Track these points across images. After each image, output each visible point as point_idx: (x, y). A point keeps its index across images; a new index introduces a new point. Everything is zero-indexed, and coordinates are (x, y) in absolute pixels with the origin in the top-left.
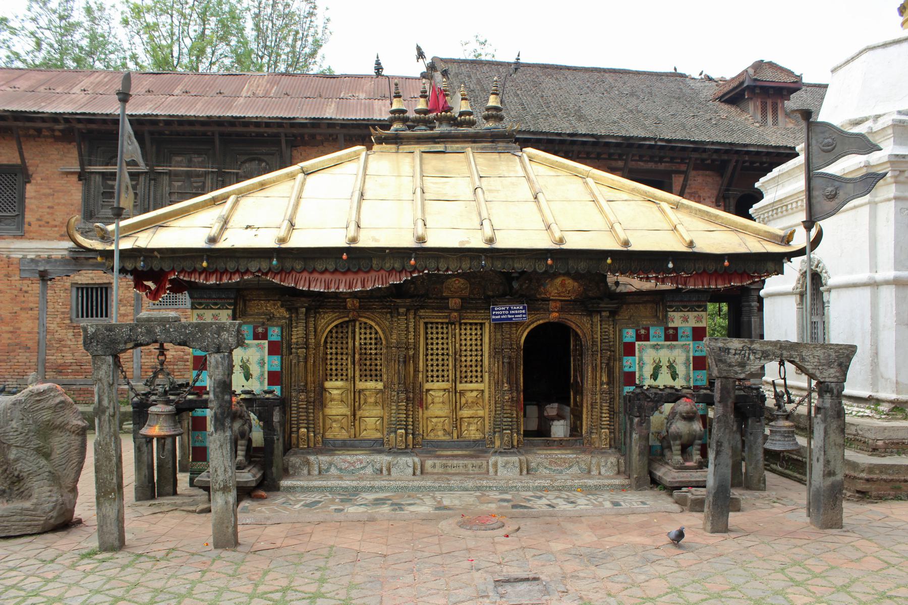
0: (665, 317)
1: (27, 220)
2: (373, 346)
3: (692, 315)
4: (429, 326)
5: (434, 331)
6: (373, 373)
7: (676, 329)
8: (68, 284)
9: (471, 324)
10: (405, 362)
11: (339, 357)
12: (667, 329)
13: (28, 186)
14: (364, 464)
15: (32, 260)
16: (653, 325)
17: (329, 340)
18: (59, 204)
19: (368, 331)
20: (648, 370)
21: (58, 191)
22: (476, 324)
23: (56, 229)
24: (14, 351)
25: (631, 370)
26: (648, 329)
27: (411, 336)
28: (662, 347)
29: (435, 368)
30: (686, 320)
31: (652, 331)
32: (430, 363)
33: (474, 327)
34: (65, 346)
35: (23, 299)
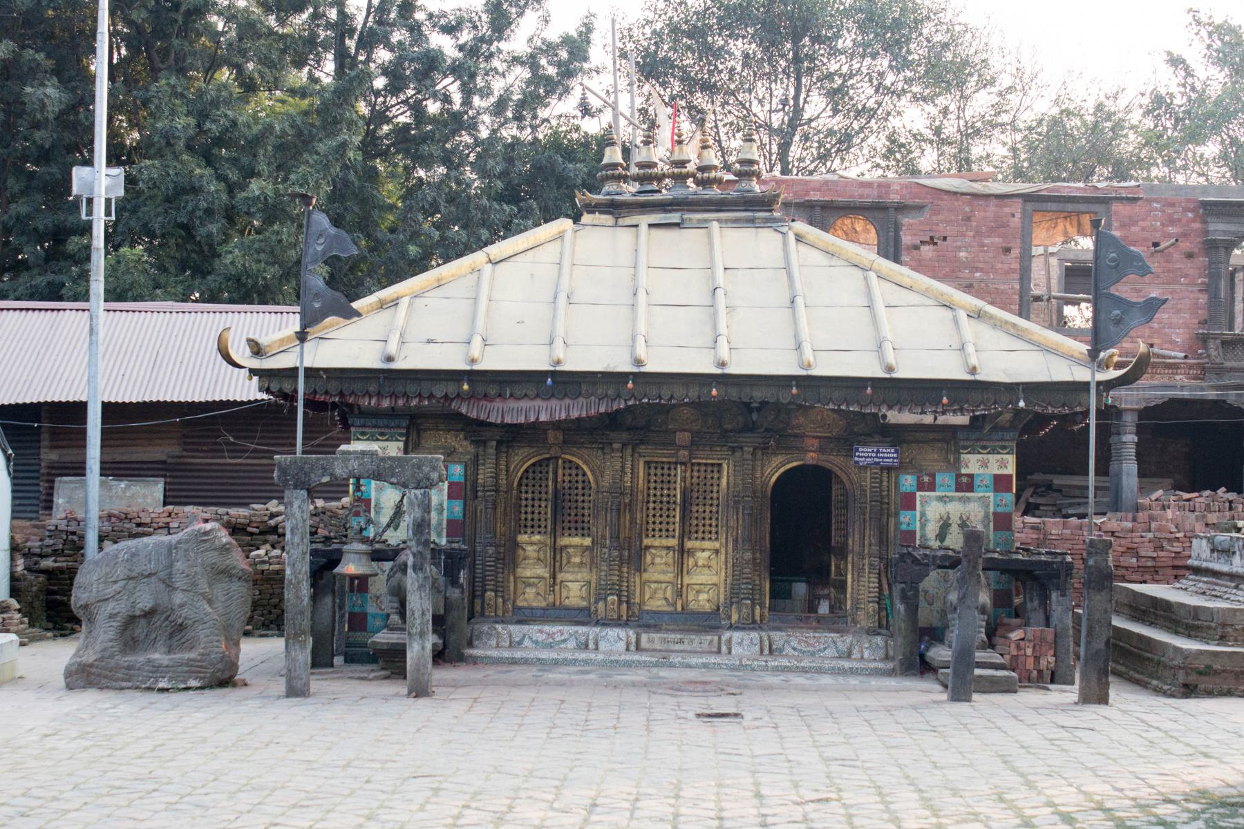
0: (958, 460)
2: (580, 491)
3: (993, 458)
4: (653, 465)
5: (659, 472)
6: (579, 525)
7: (971, 476)
9: (706, 464)
10: (619, 510)
11: (537, 503)
12: (959, 476)
14: (566, 636)
16: (940, 471)
17: (525, 481)
19: (574, 472)
20: (932, 529)
22: (713, 465)
25: (911, 528)
26: (933, 476)
27: (628, 478)
28: (952, 499)
29: (658, 520)
30: (985, 464)
31: (939, 478)
32: (651, 512)
33: (710, 469)
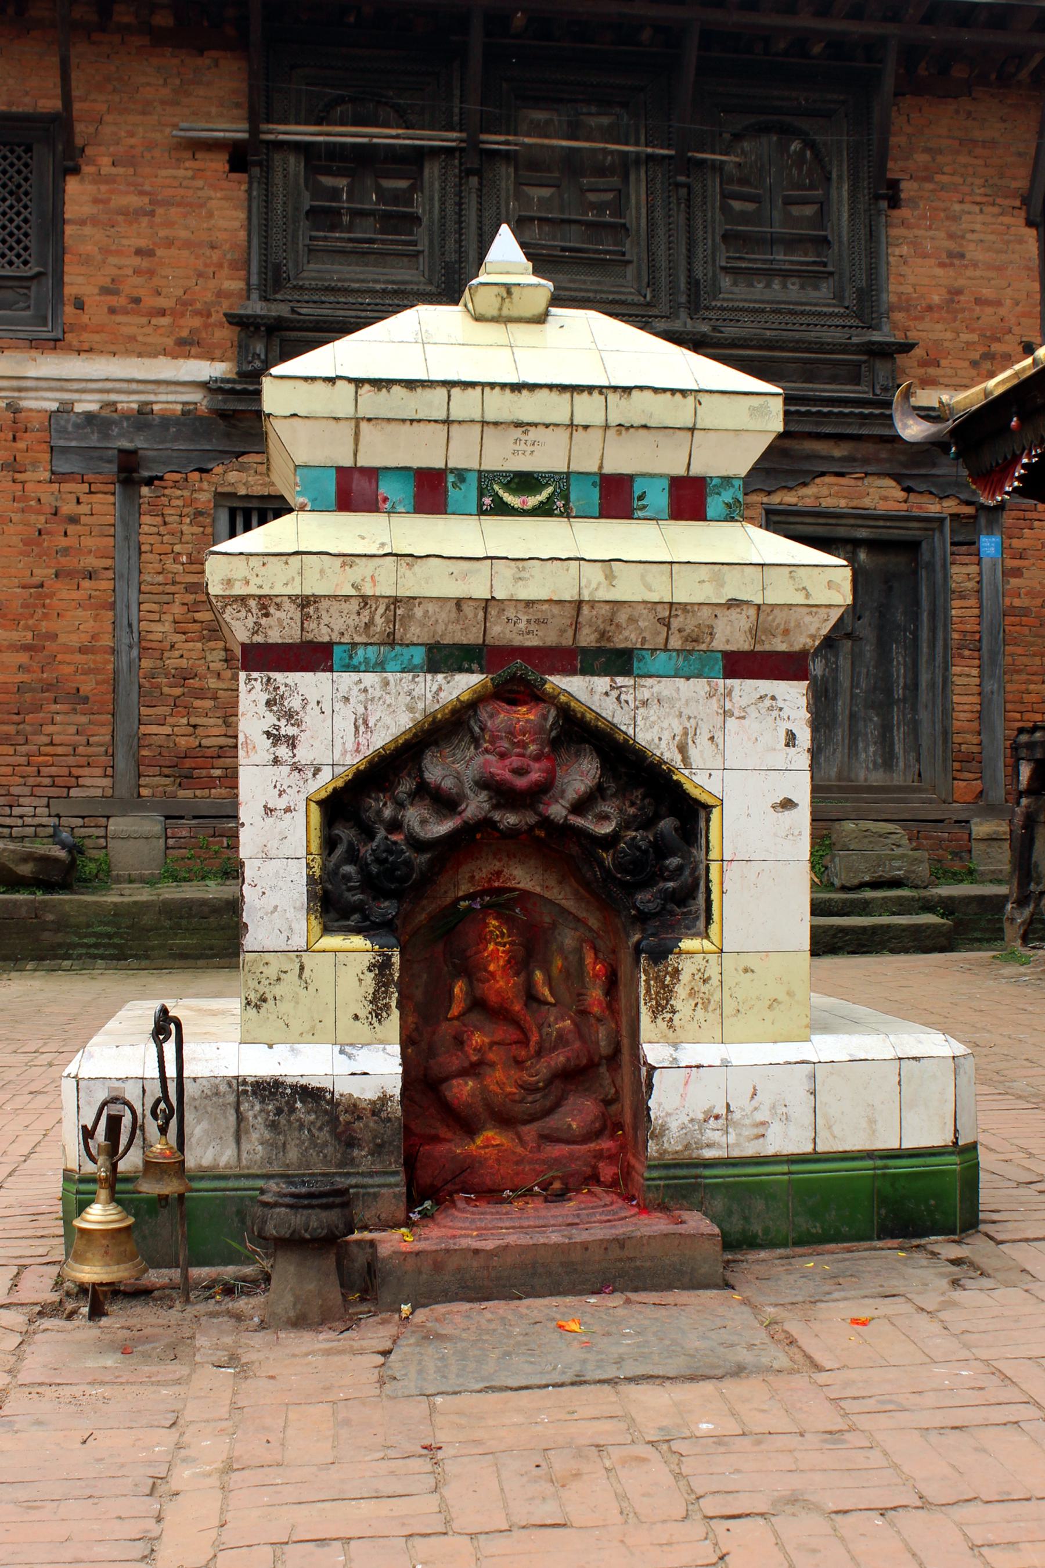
1: (69, 291)
8: (205, 498)
13: (72, 186)
18: (169, 243)
21: (167, 203)
23: (165, 321)
24: (39, 708)
34: (200, 694)
35: (64, 542)
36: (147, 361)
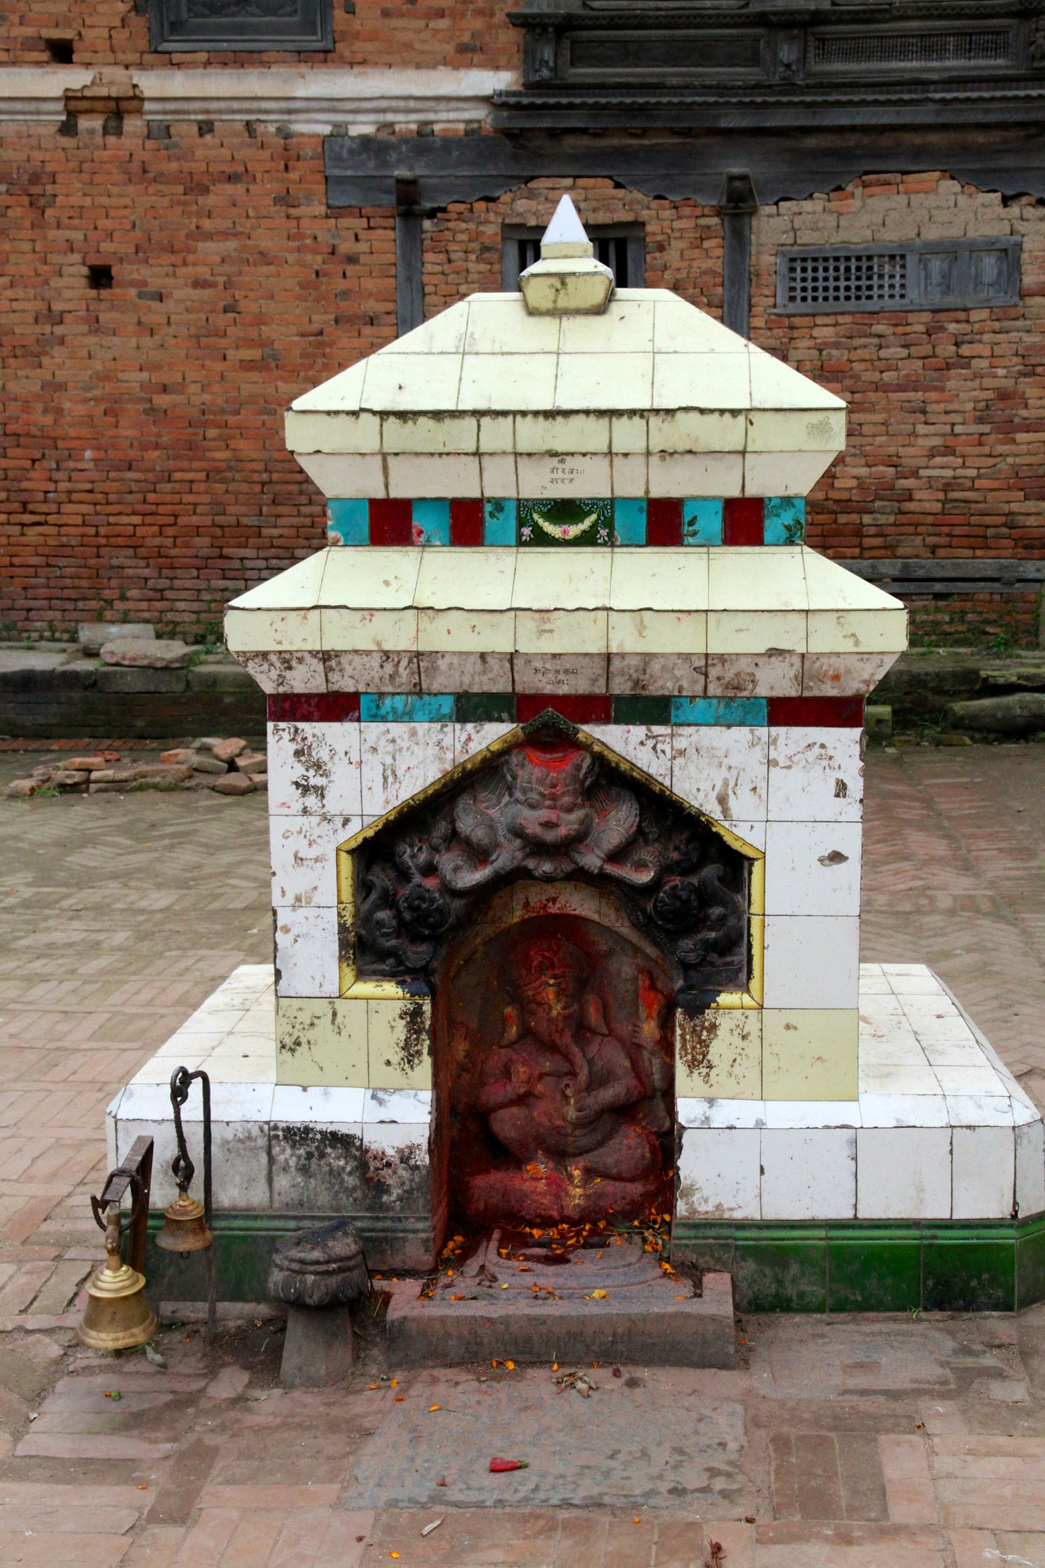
8: (492, 230)
15: (365, 141)
23: (443, 24)
35: (342, 285)
36: (424, 75)
